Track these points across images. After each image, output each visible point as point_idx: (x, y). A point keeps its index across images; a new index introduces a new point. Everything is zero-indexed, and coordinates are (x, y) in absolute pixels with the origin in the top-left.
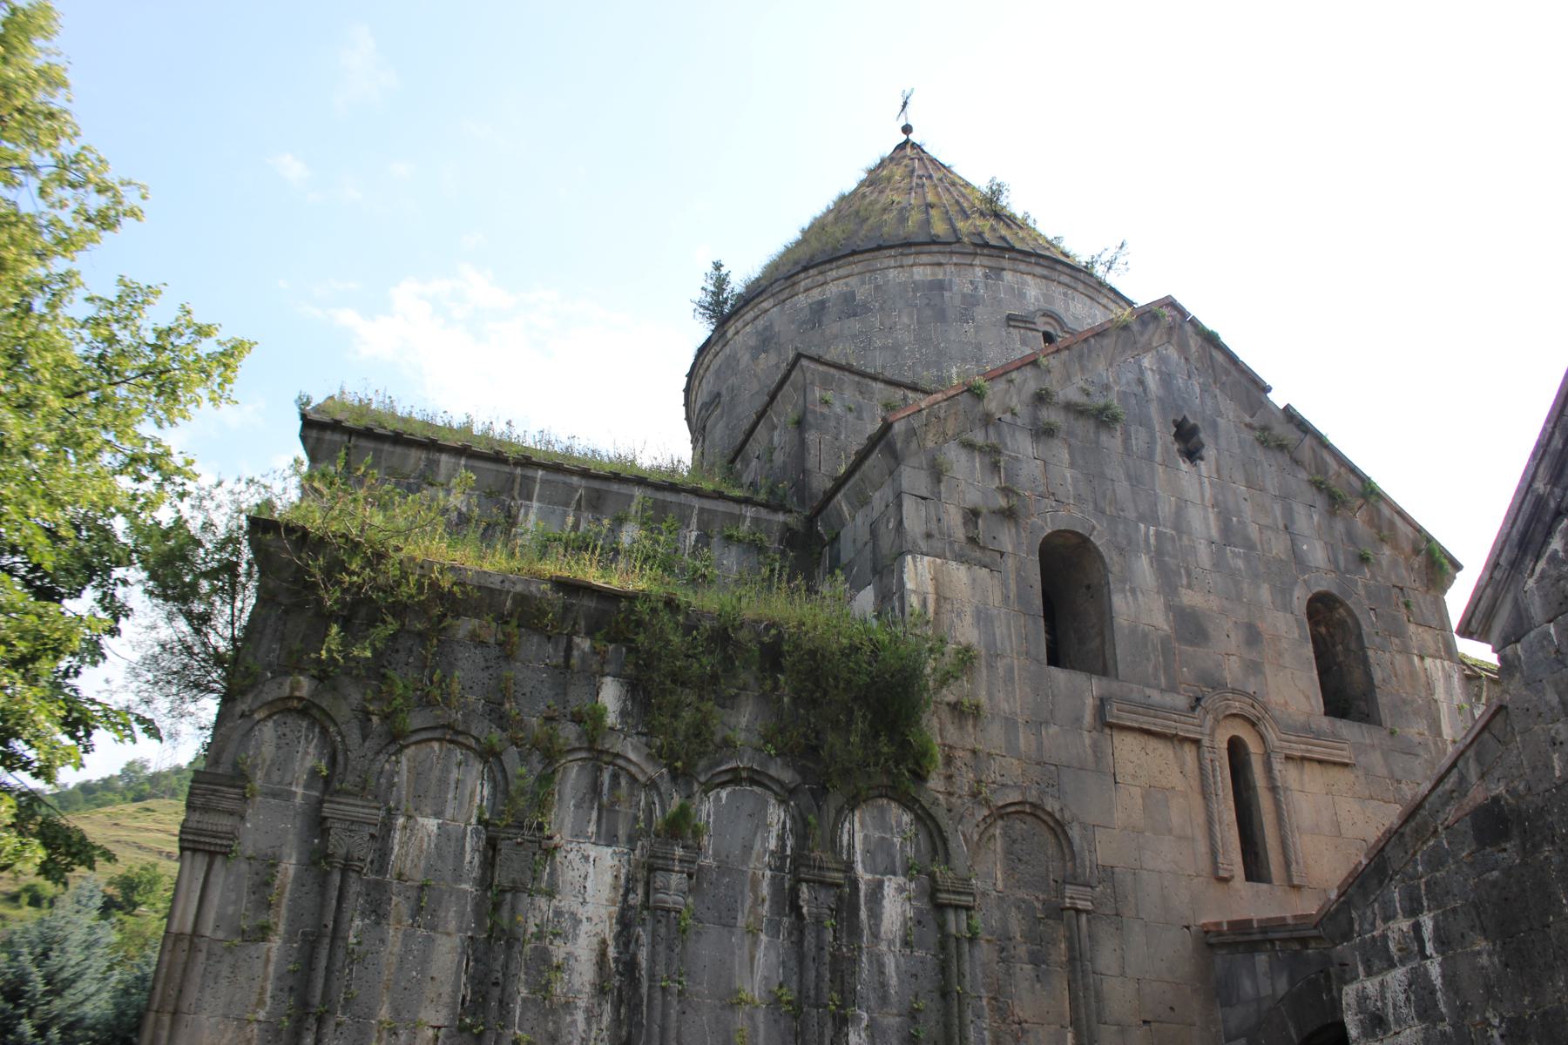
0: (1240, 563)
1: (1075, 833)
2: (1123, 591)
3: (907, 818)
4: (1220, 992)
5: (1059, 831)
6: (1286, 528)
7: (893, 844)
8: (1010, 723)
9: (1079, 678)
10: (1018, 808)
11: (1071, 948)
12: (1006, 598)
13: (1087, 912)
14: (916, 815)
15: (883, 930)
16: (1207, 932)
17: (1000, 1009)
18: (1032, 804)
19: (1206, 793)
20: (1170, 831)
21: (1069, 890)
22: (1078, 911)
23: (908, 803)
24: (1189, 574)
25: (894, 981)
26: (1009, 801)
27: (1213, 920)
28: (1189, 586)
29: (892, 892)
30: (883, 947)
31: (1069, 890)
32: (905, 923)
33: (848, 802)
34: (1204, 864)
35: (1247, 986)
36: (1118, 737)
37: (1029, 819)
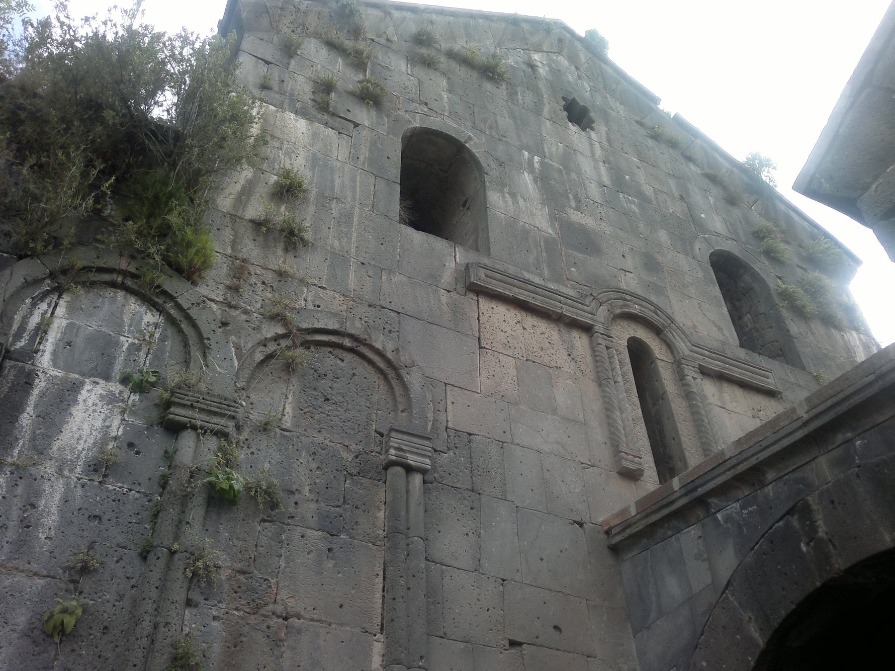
0: (634, 208)
1: (414, 379)
2: (501, 191)
3: (150, 317)
4: (636, 613)
5: (391, 374)
6: (682, 198)
7: (118, 344)
8: (339, 260)
9: (438, 243)
10: (333, 339)
11: (393, 516)
12: (354, 158)
13: (423, 471)
14: (171, 321)
15: (56, 446)
16: (607, 532)
17: (253, 590)
18: (351, 336)
19: (602, 380)
20: (554, 411)
21: (396, 440)
22: (409, 469)
23: (154, 297)
24: (578, 201)
25: (52, 519)
26: (318, 325)
27: (618, 508)
28: (578, 209)
29: (93, 398)
30: (49, 468)
31: (396, 440)
32: (105, 437)
33: (52, 275)
34: (604, 455)
35: (673, 587)
36: (485, 305)
37: (348, 357)
